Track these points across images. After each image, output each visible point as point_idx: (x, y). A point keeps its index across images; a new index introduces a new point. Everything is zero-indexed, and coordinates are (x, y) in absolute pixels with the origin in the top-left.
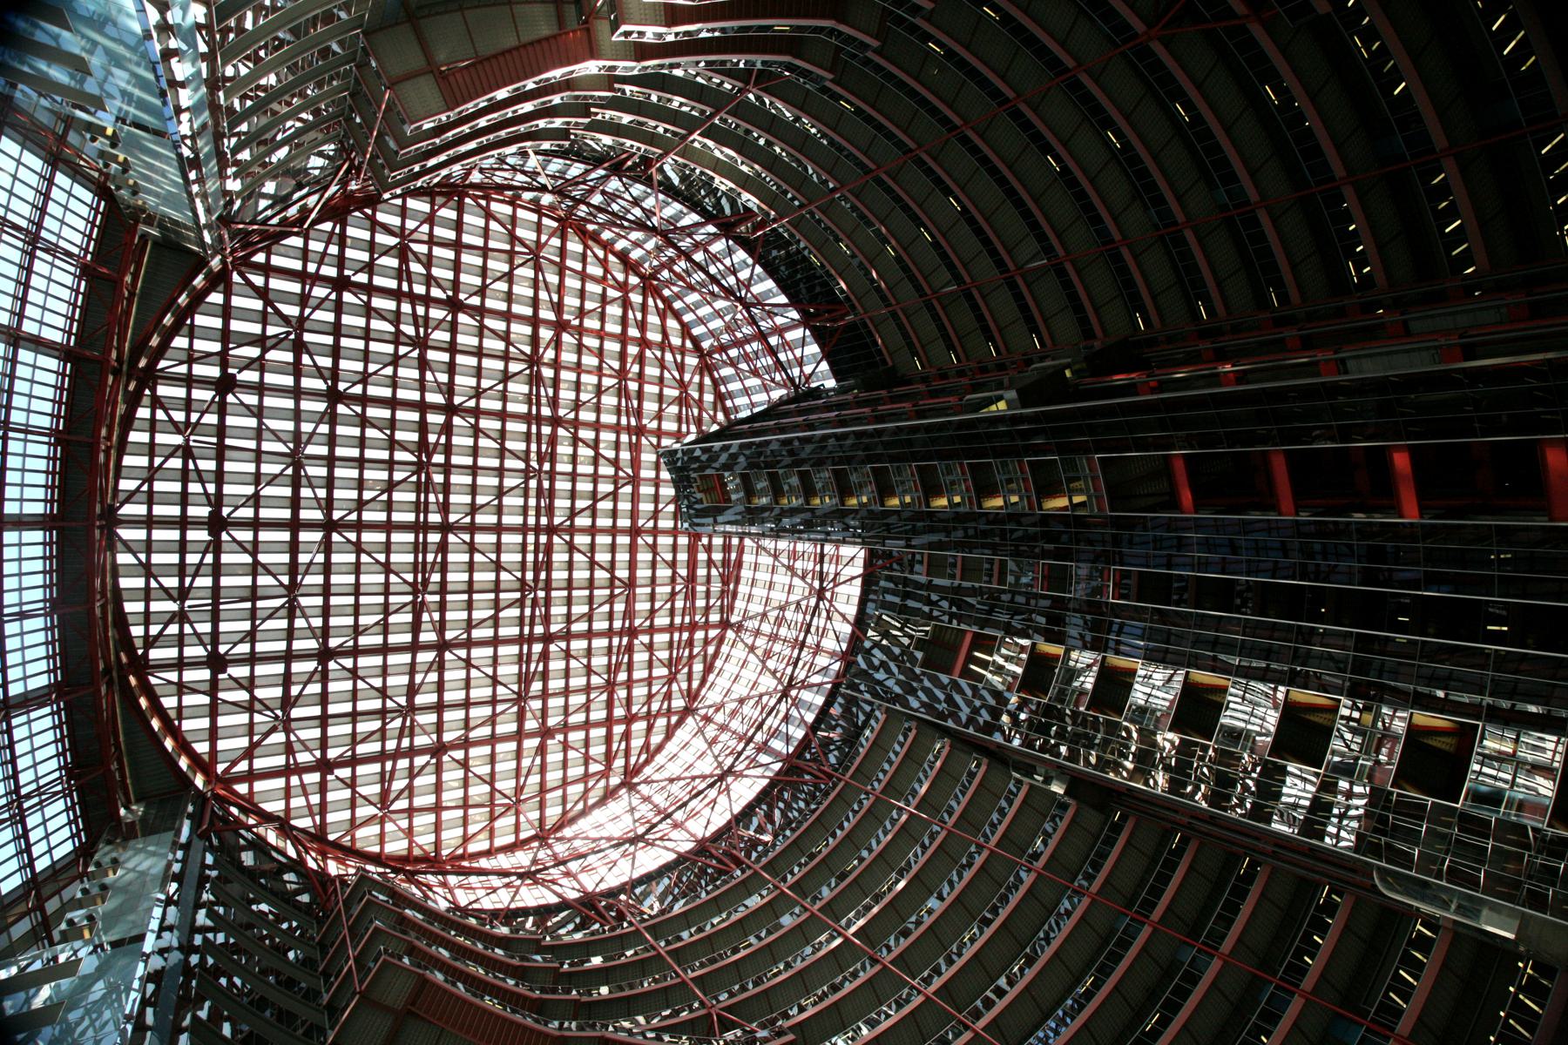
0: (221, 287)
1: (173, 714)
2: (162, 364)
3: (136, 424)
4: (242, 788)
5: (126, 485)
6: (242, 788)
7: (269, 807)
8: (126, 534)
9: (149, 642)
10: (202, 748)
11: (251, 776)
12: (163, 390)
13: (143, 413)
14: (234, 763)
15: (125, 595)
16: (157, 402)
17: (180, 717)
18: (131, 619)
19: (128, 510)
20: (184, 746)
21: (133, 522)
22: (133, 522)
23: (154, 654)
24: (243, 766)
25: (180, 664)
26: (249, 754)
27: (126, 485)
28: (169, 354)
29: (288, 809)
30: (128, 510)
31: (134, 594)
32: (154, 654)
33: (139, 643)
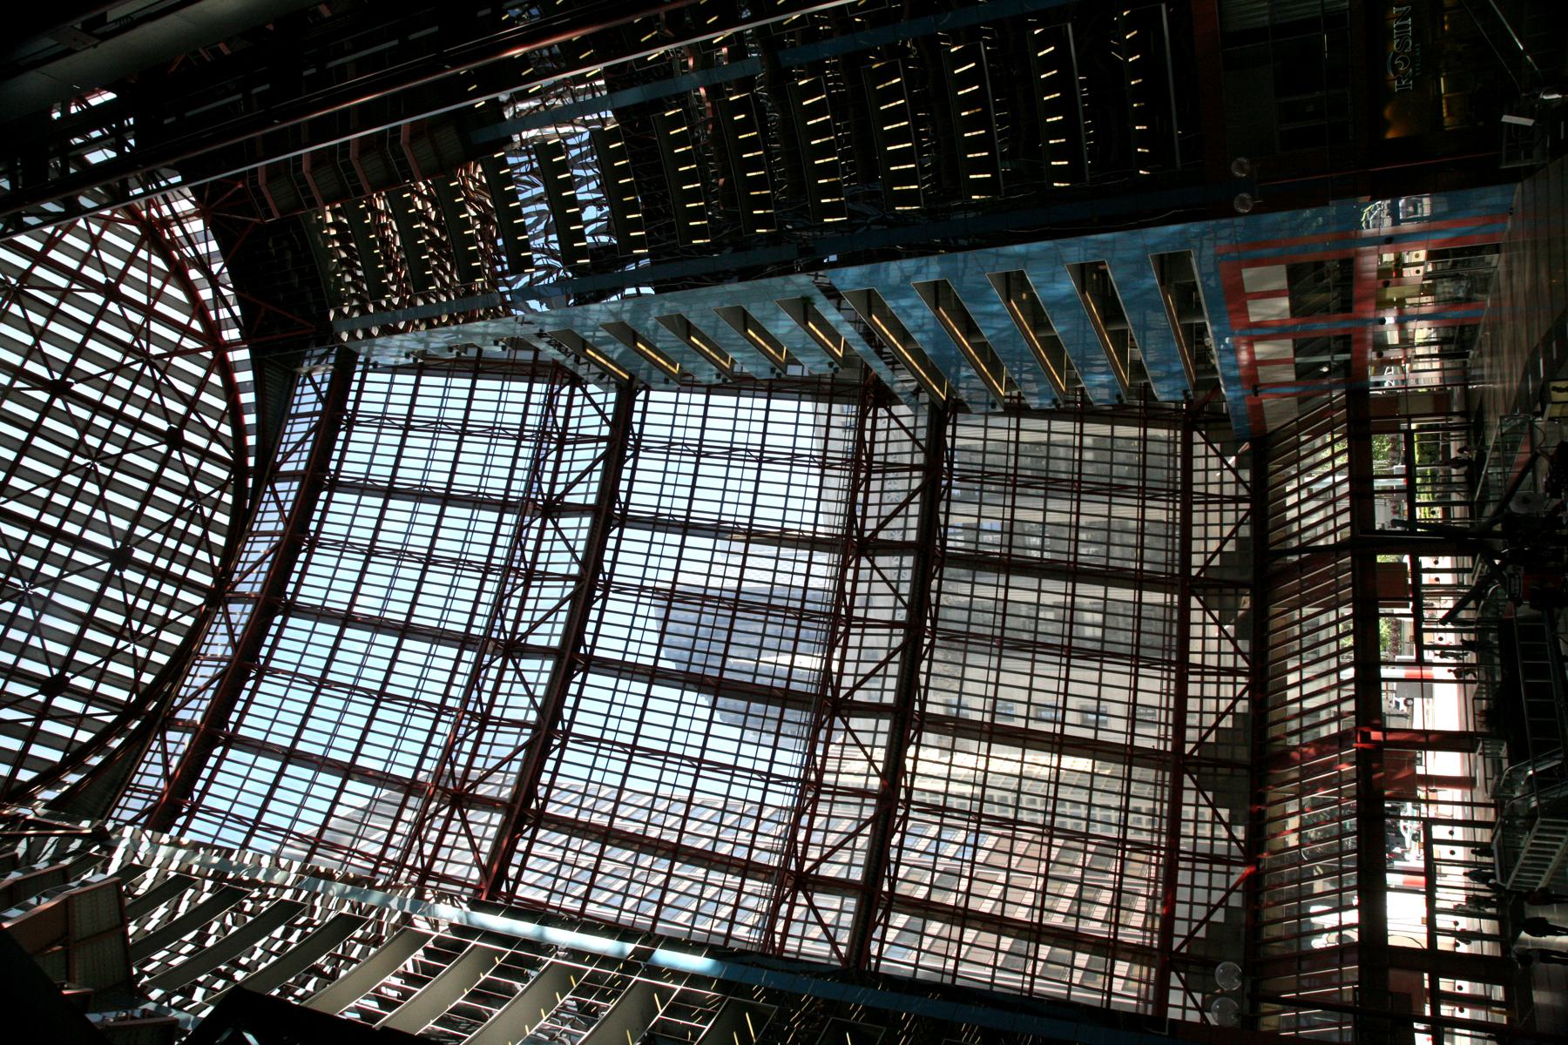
0: (15, 785)
1: (227, 419)
2: (110, 719)
3: (157, 670)
4: (196, 325)
5: (188, 621)
6: (196, 325)
7: (180, 295)
8: (207, 581)
9: (222, 486)
10: (215, 379)
11: (185, 331)
12: (122, 695)
13: (147, 678)
14: (196, 351)
15: (225, 531)
16: (133, 685)
17: (224, 413)
18: (228, 510)
19: (197, 600)
20: (231, 391)
21: (195, 587)
22: (195, 587)
23: (223, 474)
24: (189, 344)
25: (205, 455)
26: (179, 351)
27: (188, 621)
28: (99, 728)
29: (165, 282)
30: (197, 600)
31: (218, 528)
32: (223, 474)
33: (230, 488)
